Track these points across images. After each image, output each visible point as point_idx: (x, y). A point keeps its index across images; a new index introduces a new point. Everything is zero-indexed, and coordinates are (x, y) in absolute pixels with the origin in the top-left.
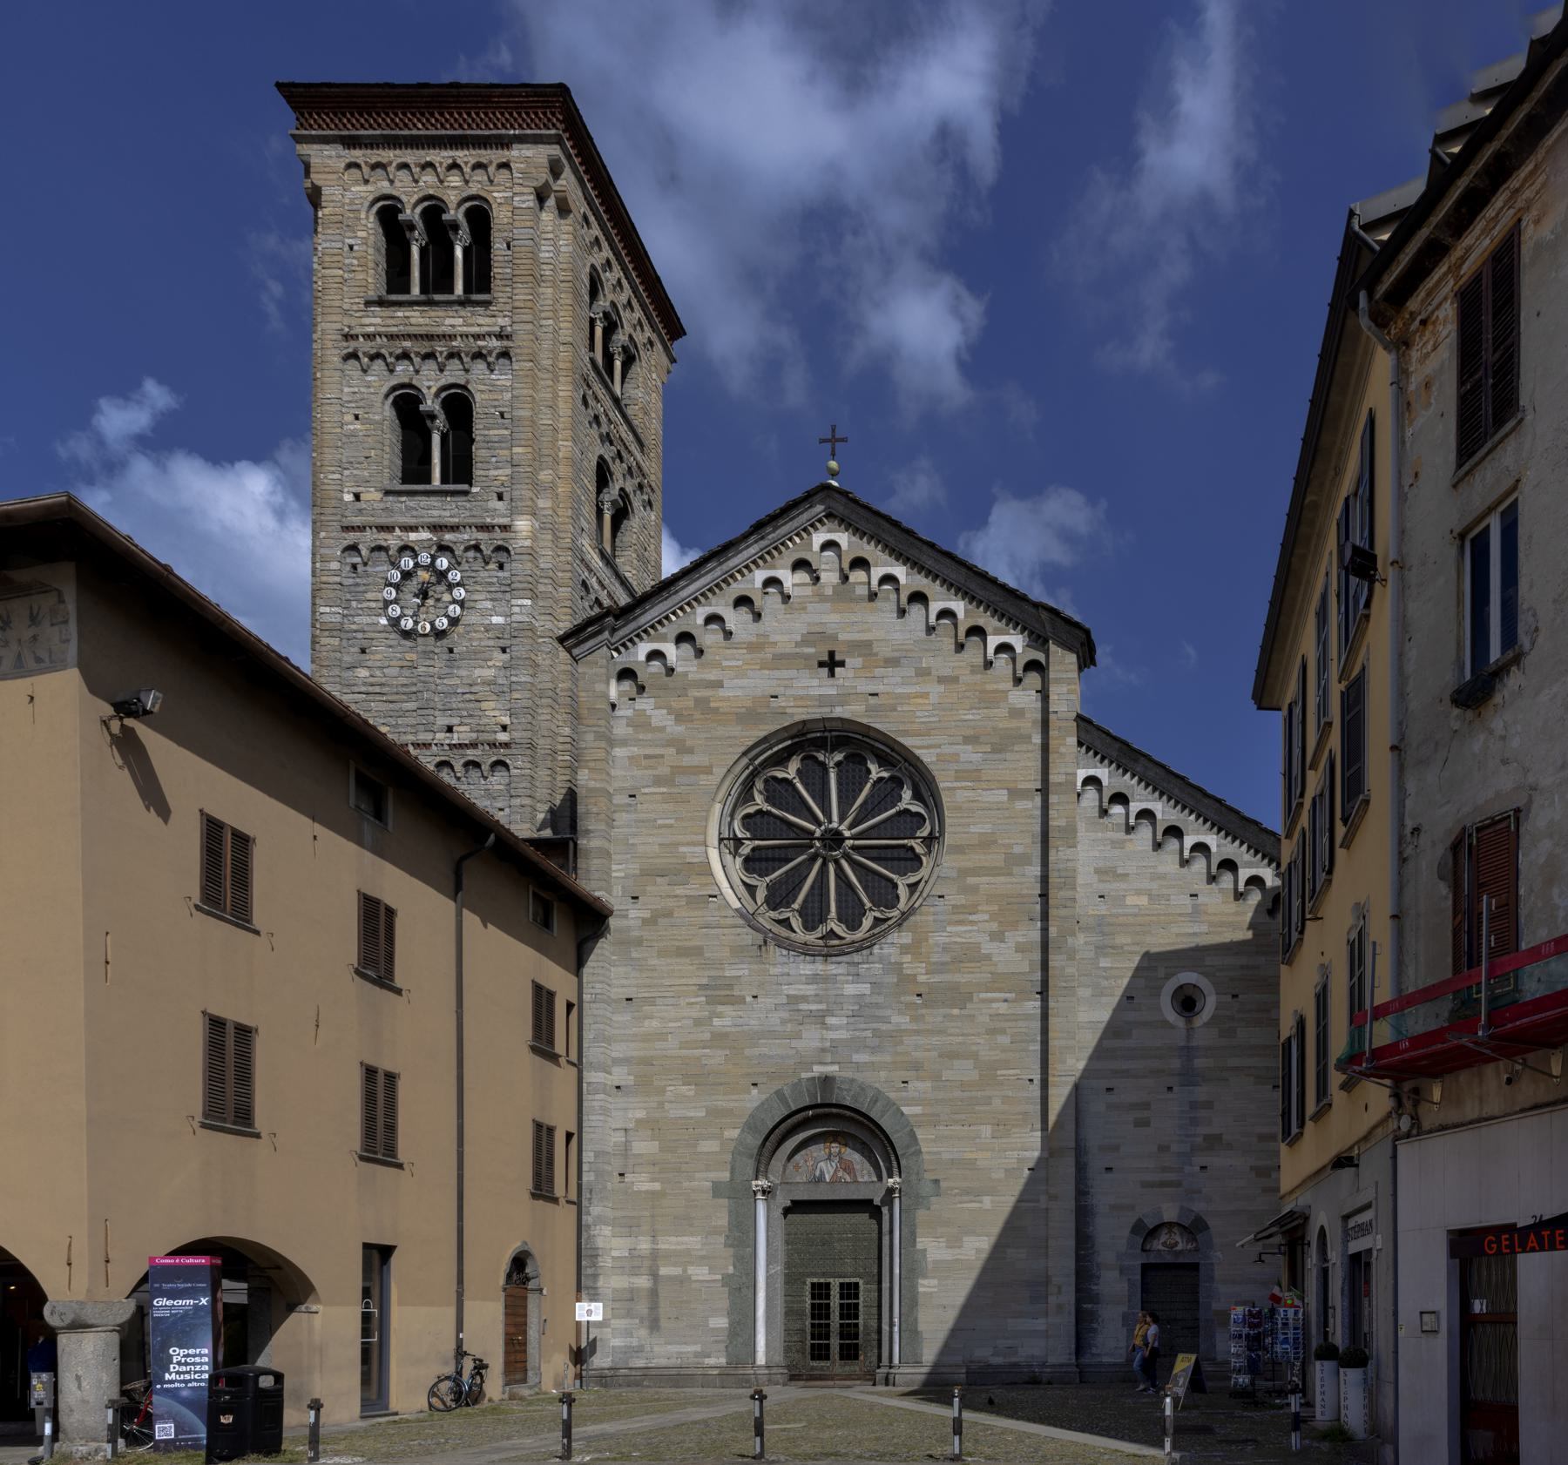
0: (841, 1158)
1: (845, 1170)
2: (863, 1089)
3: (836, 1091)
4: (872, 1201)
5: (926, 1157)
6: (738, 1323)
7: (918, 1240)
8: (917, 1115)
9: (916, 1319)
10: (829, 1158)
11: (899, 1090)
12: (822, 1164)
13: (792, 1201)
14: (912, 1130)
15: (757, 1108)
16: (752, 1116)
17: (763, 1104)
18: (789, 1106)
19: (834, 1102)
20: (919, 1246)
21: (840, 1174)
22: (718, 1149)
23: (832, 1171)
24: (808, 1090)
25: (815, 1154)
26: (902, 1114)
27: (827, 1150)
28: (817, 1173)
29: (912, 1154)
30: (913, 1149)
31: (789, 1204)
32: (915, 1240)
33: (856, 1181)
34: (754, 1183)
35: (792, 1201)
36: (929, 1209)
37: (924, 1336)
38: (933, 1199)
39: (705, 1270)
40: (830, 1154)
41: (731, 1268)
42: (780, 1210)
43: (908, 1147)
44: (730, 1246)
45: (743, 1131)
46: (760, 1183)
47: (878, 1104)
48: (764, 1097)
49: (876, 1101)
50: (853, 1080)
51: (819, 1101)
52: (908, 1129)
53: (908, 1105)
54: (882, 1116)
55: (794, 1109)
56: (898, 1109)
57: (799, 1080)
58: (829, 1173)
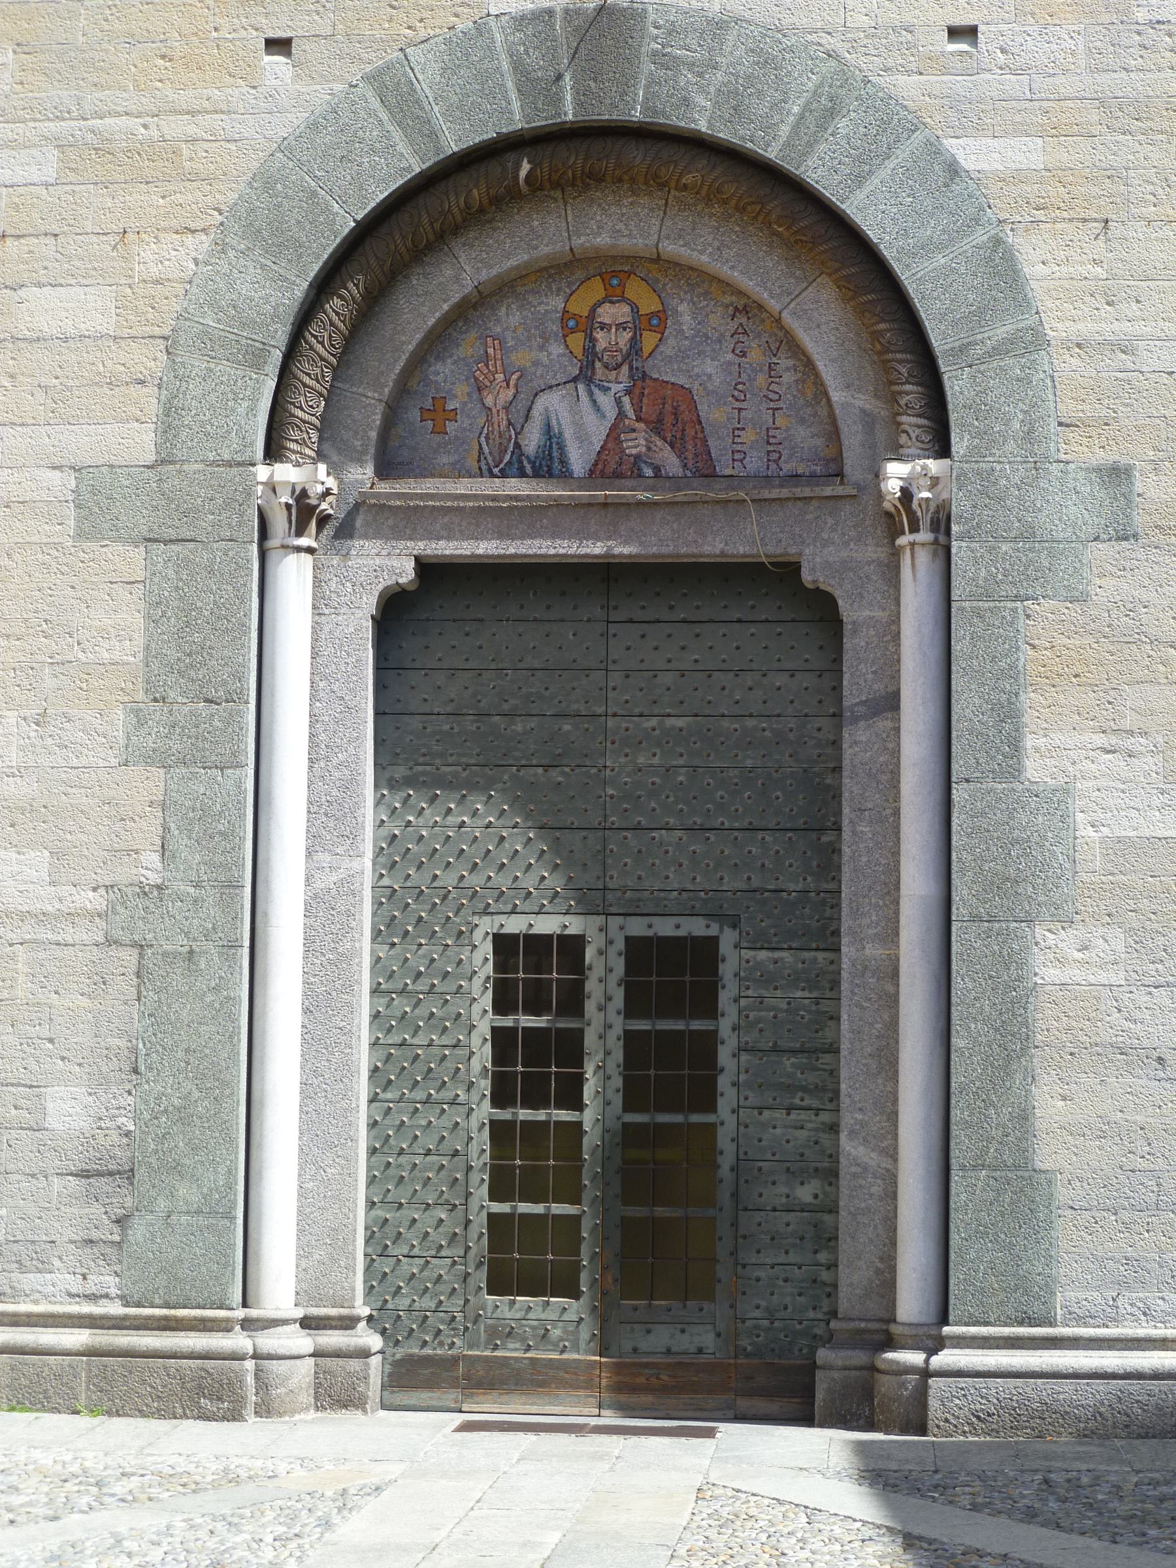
0: (640, 378)
1: (657, 427)
2: (768, 63)
3: (647, 67)
4: (793, 568)
5: (1068, 364)
6: (183, 1116)
7: (1029, 742)
8: (1018, 177)
9: (1024, 1117)
10: (585, 376)
11: (936, 64)
12: (554, 404)
13: (424, 567)
14: (998, 241)
15: (284, 147)
16: (266, 181)
17: (314, 127)
18: (433, 136)
19: (637, 114)
20: (1035, 769)
21: (635, 444)
22: (107, 324)
23: (598, 431)
24: (518, 66)
25: (521, 358)
26: (953, 170)
27: (577, 341)
28: (532, 441)
29: (997, 351)
30: (1001, 332)
31: (405, 573)
32: (1016, 745)
33: (707, 472)
34: (263, 472)
35: (424, 567)
36: (1082, 599)
37: (1062, 1194)
38: (1103, 552)
39: (38, 862)
40: (591, 355)
41: (154, 859)
42: (369, 604)
43: (981, 315)
44: (159, 759)
45: (221, 247)
46: (287, 473)
47: (842, 125)
48: (320, 94)
49: (832, 113)
50: (718, 27)
51: (569, 113)
52: (980, 236)
53: (979, 130)
54: (860, 180)
55: (453, 142)
56: (934, 149)
57: (480, 28)
58: (582, 438)
